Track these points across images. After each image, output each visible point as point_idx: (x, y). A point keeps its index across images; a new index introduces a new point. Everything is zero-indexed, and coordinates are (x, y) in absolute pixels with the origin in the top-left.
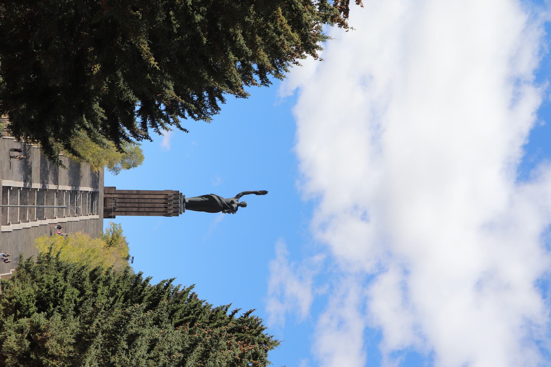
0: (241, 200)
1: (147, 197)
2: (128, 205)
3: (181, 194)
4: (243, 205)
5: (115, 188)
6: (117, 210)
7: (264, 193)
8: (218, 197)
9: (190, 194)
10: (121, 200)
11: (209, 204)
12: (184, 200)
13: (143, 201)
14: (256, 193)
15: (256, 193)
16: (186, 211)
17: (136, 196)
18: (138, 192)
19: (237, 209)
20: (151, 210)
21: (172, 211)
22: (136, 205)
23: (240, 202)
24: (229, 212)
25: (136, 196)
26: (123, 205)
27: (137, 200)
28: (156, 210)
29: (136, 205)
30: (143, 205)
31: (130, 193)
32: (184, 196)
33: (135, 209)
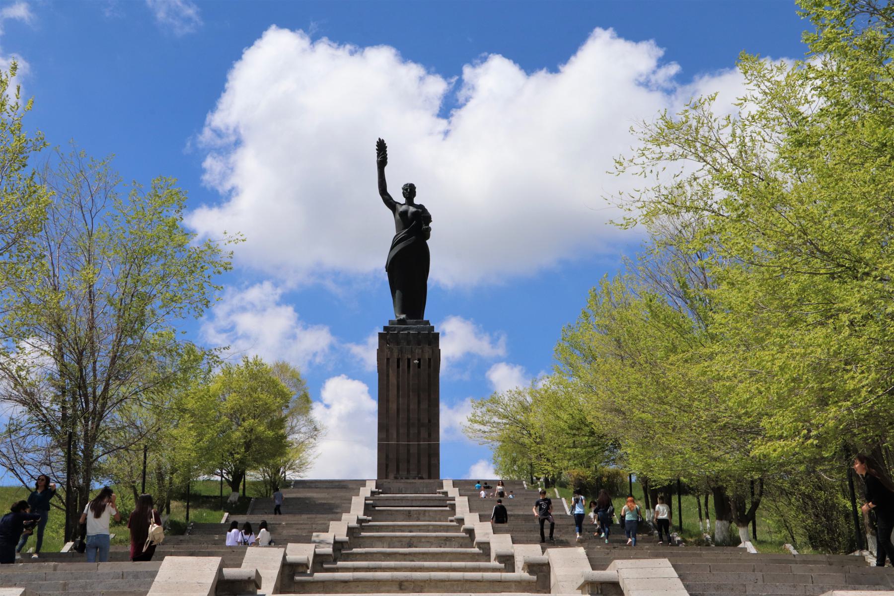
0: (398, 197)
1: (393, 406)
2: (413, 450)
3: (385, 328)
4: (410, 191)
7: (381, 147)
8: (392, 249)
12: (401, 322)
14: (382, 162)
15: (382, 162)
16: (425, 318)
19: (421, 207)
21: (427, 348)
22: (413, 431)
24: (428, 219)
27: (401, 431)
29: (413, 431)
33: (424, 433)
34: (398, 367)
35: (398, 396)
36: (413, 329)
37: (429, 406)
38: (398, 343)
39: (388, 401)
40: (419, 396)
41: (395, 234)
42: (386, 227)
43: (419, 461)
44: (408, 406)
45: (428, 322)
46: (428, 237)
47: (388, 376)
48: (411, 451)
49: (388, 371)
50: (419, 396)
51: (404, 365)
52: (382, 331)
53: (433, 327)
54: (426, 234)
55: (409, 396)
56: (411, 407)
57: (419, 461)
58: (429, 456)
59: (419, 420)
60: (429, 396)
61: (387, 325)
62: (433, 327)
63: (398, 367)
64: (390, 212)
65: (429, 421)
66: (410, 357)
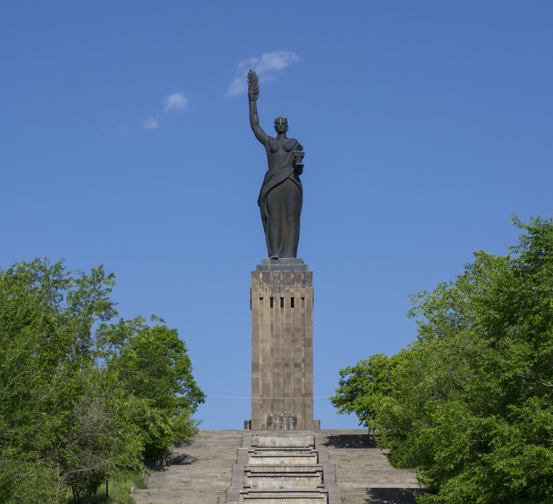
23: (274, 134)
34: (272, 306)
36: (286, 268)
51: (277, 303)
63: (272, 306)
66: (283, 296)
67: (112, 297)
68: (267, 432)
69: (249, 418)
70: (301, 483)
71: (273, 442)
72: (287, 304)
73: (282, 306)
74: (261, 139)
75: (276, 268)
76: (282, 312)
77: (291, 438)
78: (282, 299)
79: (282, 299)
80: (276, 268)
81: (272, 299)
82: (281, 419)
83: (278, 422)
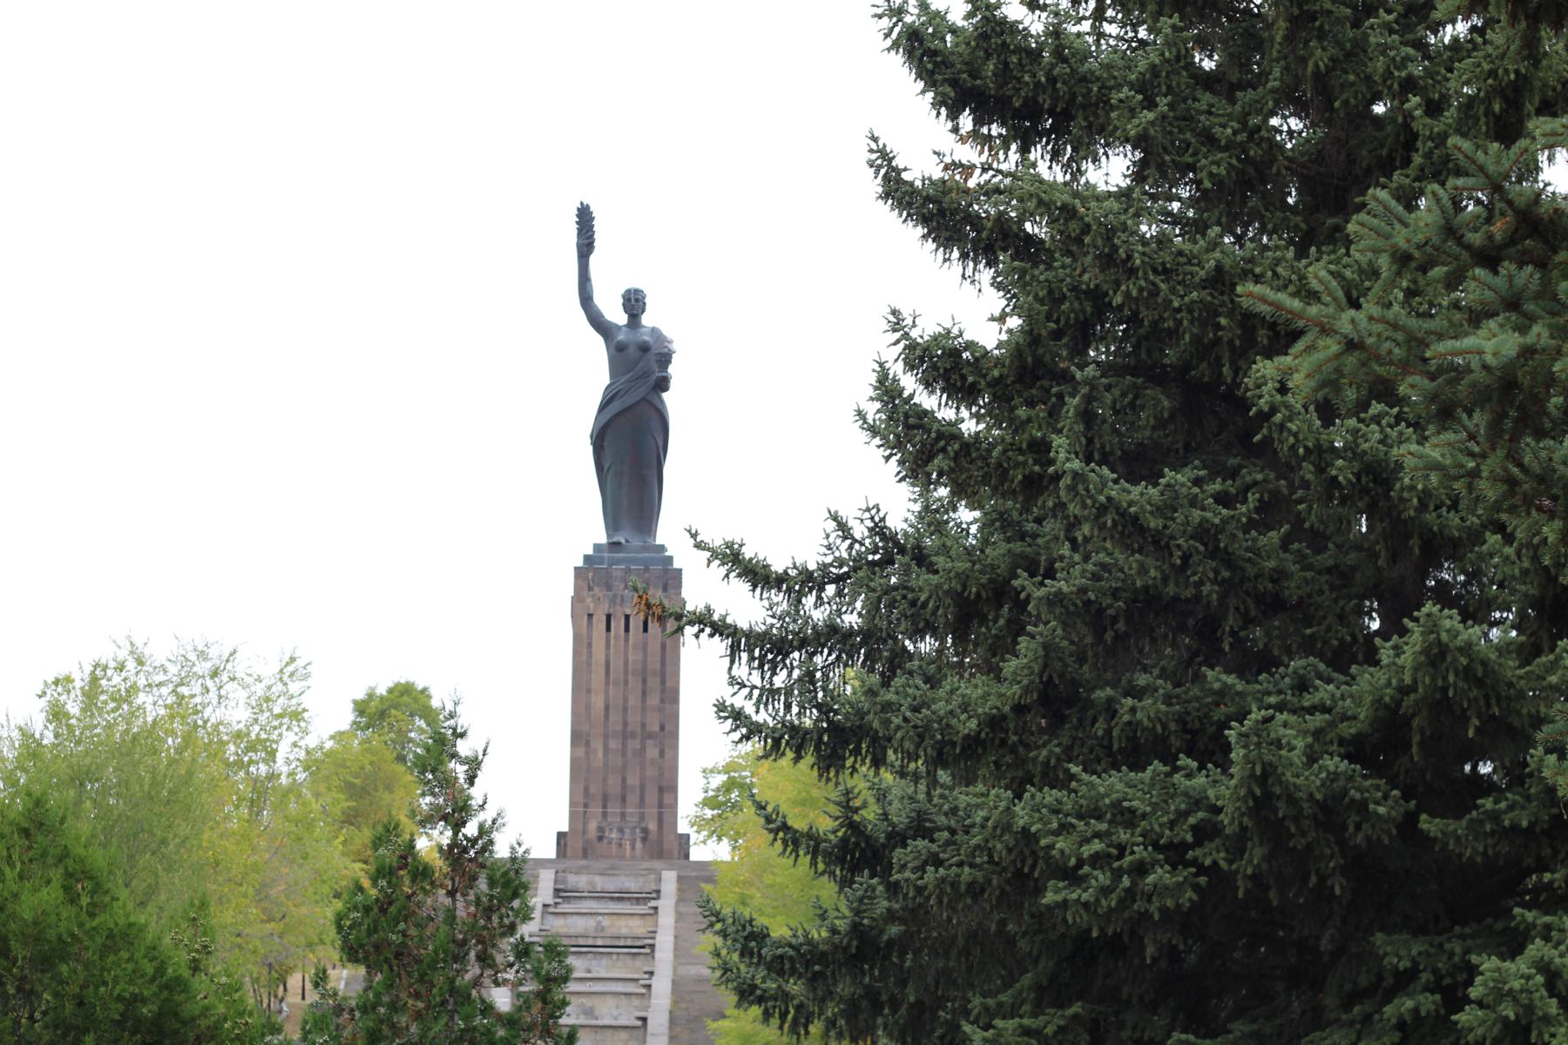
0: (618, 316)
1: (598, 701)
2: (633, 780)
3: (587, 558)
4: (634, 303)
5: (561, 836)
6: (652, 826)
7: (585, 218)
8: (603, 407)
9: (584, 523)
10: (613, 809)
11: (630, 442)
12: (614, 546)
13: (615, 718)
14: (586, 246)
15: (586, 246)
17: (597, 745)
18: (579, 737)
19: (654, 331)
20: (653, 682)
24: (665, 359)
25: (597, 745)
26: (633, 798)
28: (654, 663)
30: (634, 719)
31: (579, 771)
32: (597, 547)
33: (652, 752)
34: (608, 629)
35: (607, 683)
36: (634, 561)
37: (662, 701)
38: (609, 588)
39: (589, 691)
40: (644, 682)
41: (607, 382)
42: (591, 372)
43: (642, 799)
44: (626, 700)
45: (662, 548)
46: (666, 389)
47: (590, 645)
48: (629, 782)
49: (590, 637)
50: (644, 682)
51: (618, 625)
52: (580, 564)
53: (671, 558)
54: (663, 384)
55: (626, 682)
56: (631, 702)
57: (642, 799)
58: (661, 790)
59: (643, 726)
60: (663, 682)
61: (590, 552)
62: (671, 558)
63: (608, 629)
64: (598, 341)
65: (662, 728)
66: (628, 612)
67: (307, 701)
68: (584, 862)
69: (565, 828)
70: (620, 964)
71: (591, 883)
72: (636, 627)
73: (627, 629)
74: (597, 322)
75: (618, 562)
76: (627, 640)
77: (622, 878)
78: (627, 617)
79: (627, 617)
80: (618, 562)
81: (609, 617)
82: (621, 830)
83: (614, 835)
